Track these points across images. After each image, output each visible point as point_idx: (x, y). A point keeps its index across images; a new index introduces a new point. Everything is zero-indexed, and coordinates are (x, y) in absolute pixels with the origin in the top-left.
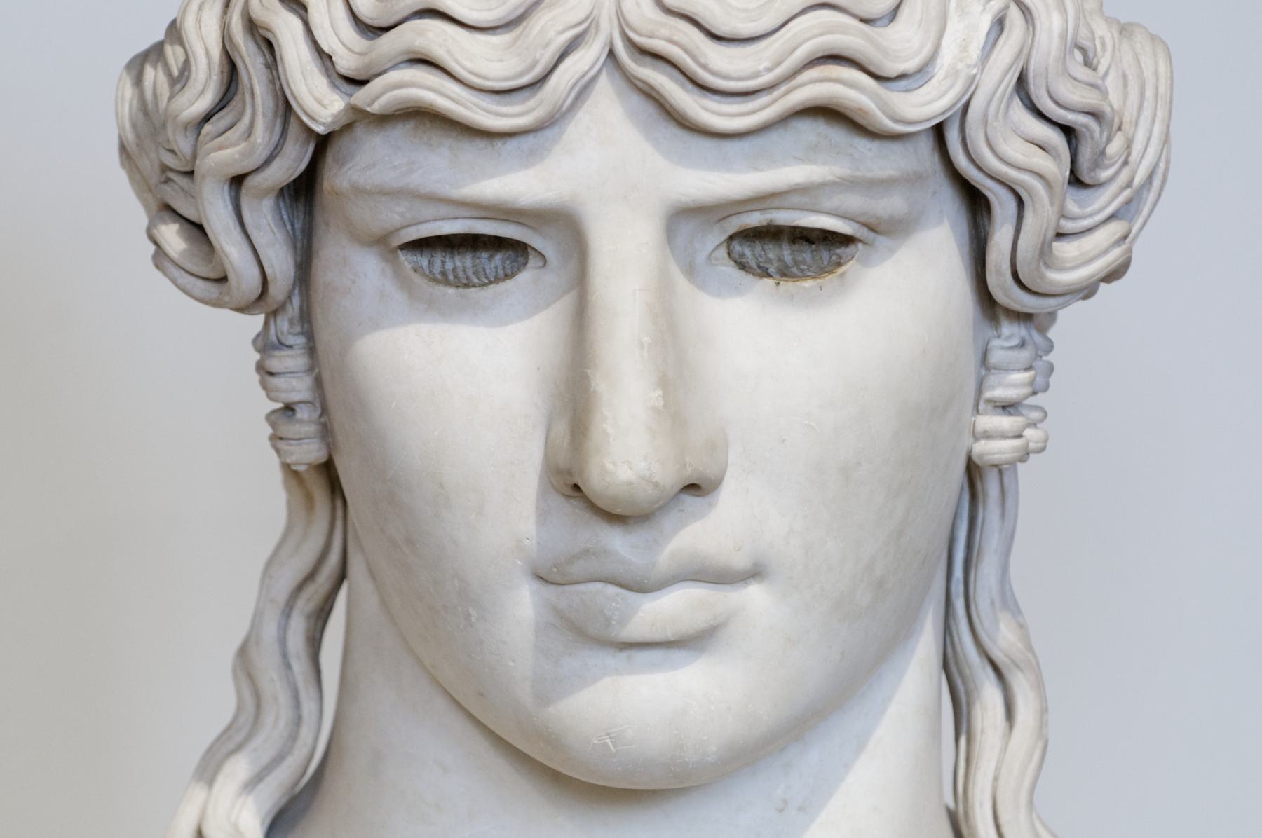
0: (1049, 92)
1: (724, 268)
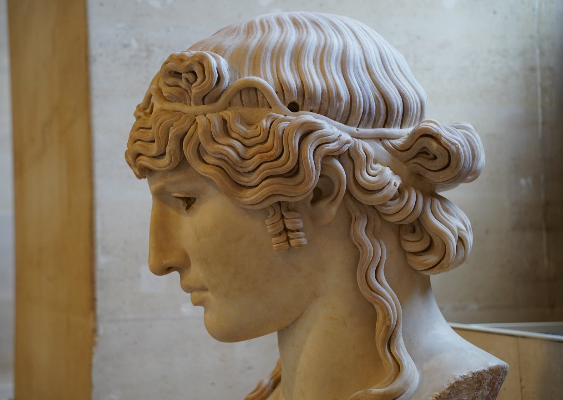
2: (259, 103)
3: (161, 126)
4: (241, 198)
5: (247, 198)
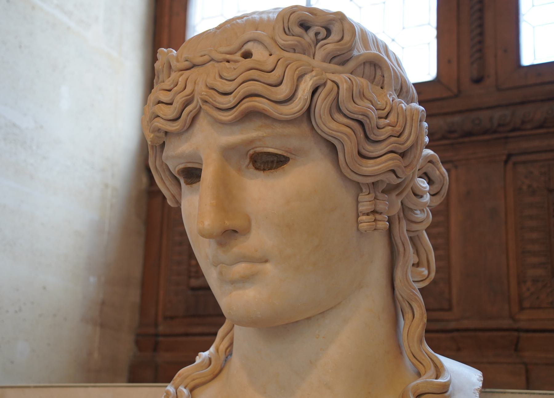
0: (346, 108)
1: (251, 170)
2: (376, 80)
3: (298, 70)
4: (361, 166)
5: (368, 167)
